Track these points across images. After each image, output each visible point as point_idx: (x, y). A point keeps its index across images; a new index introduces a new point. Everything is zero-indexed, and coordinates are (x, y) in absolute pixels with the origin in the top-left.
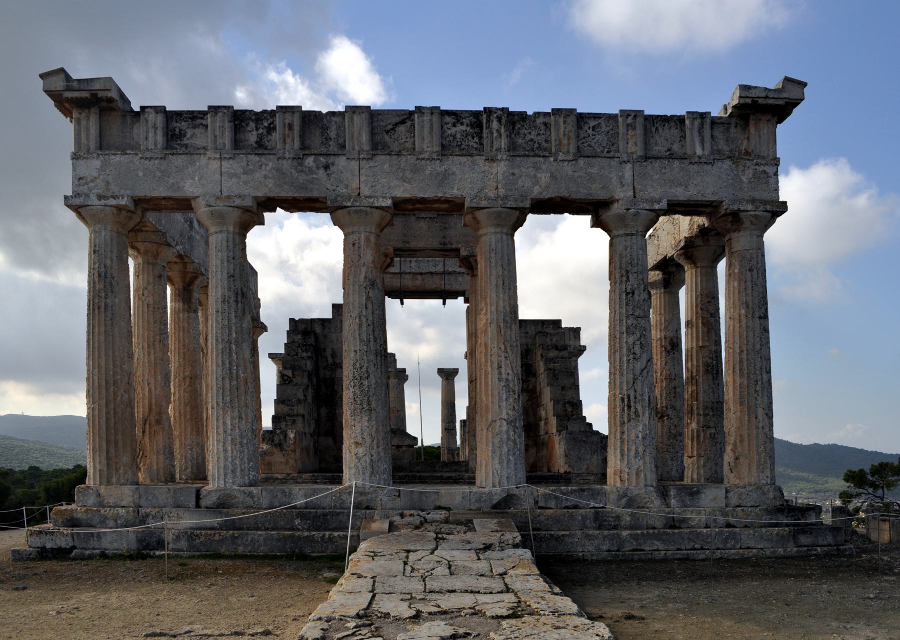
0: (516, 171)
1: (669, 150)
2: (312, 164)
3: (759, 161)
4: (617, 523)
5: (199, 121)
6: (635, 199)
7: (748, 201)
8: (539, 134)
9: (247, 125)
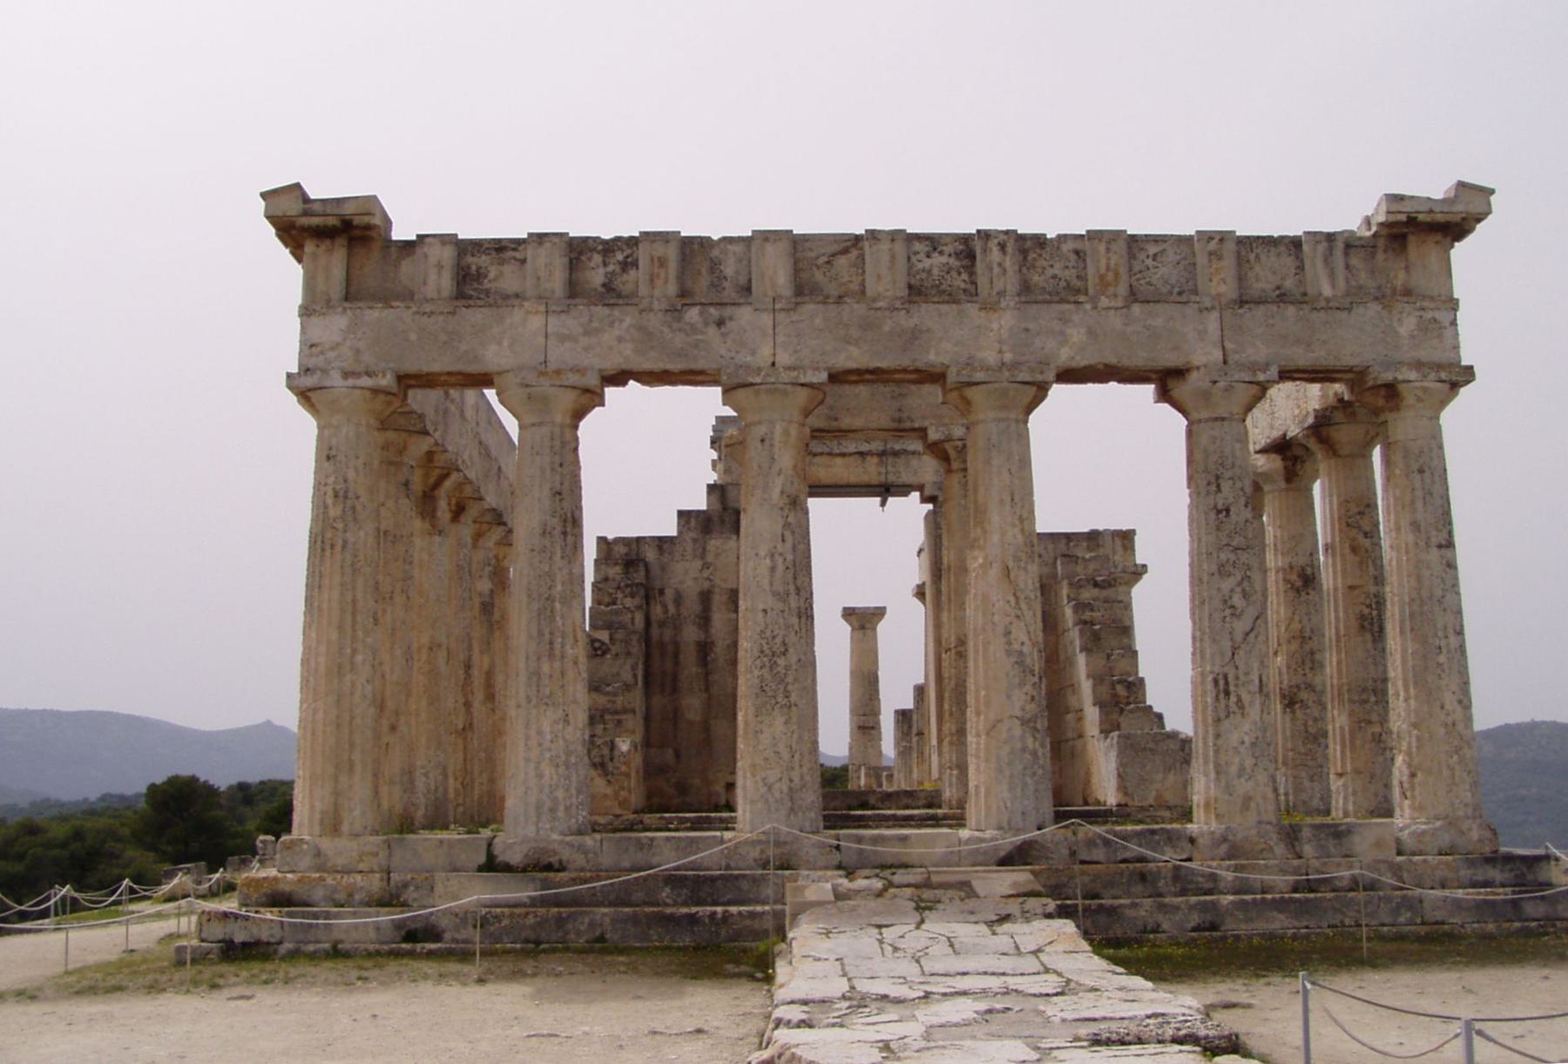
0: (1031, 326)
1: (1278, 288)
3: (1426, 304)
5: (511, 253)
9: (590, 259)
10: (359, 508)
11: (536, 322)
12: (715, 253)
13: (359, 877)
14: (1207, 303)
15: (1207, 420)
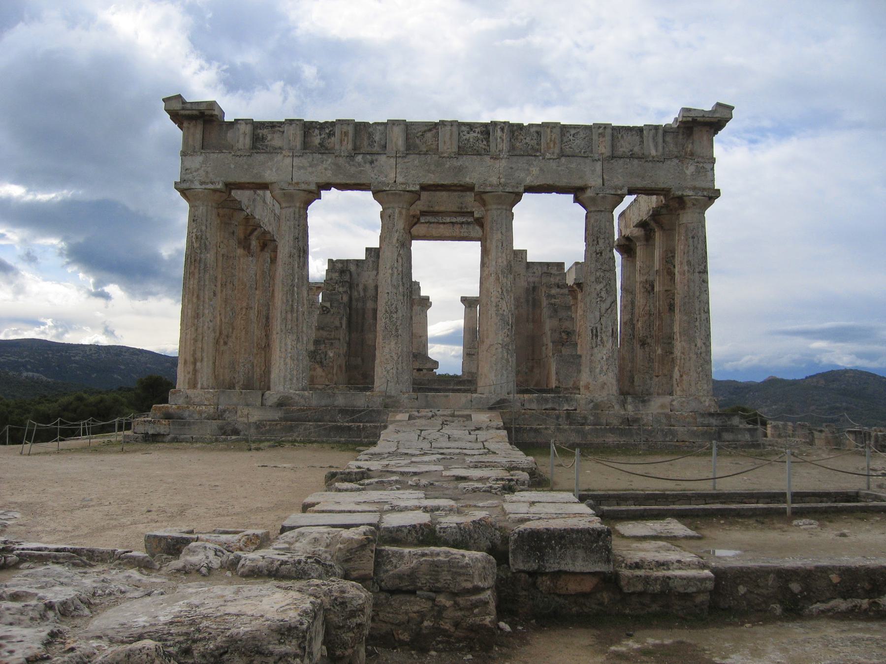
0: (513, 166)
1: (631, 151)
2: (360, 160)
4: (584, 421)
6: (604, 187)
7: (690, 189)
8: (532, 139)
9: (313, 132)
10: (207, 243)
11: (288, 161)
12: (371, 130)
13: (204, 407)
14: (596, 157)
15: (595, 211)
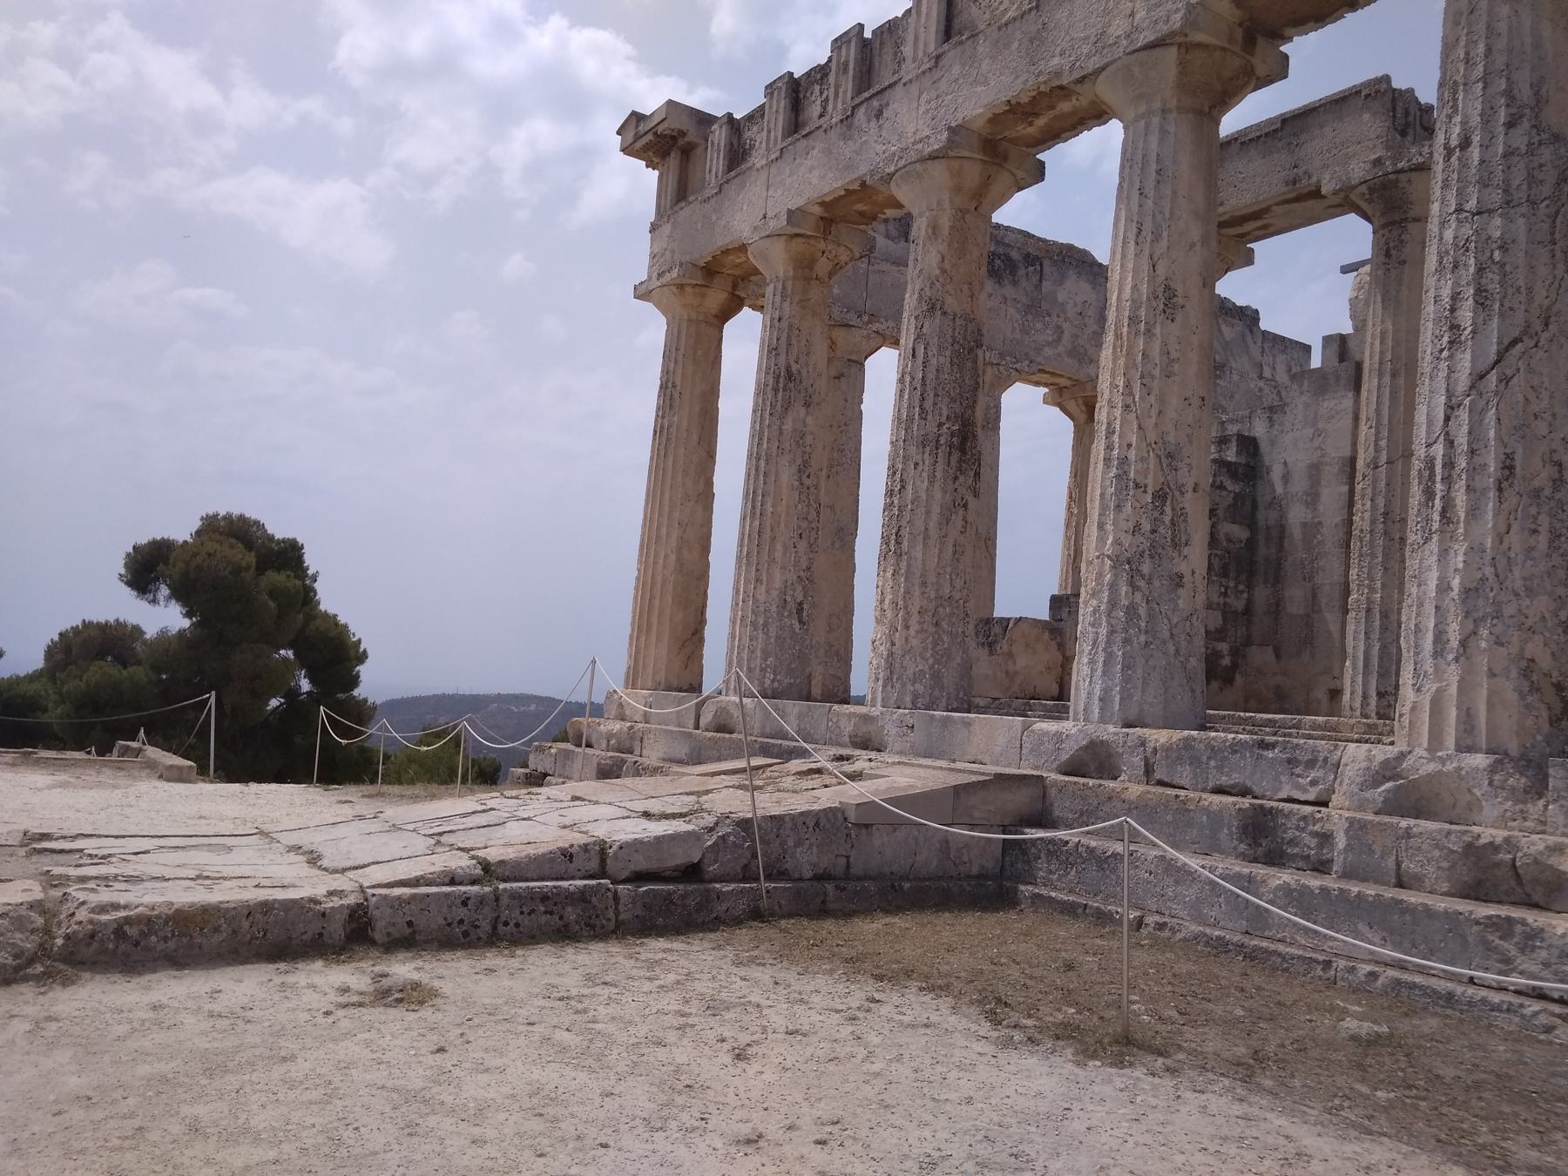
10: (676, 395)
